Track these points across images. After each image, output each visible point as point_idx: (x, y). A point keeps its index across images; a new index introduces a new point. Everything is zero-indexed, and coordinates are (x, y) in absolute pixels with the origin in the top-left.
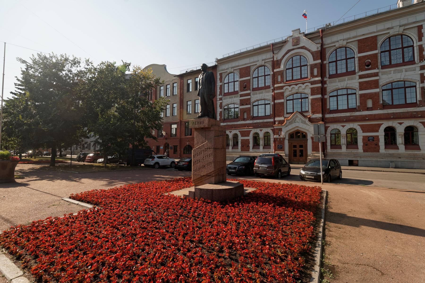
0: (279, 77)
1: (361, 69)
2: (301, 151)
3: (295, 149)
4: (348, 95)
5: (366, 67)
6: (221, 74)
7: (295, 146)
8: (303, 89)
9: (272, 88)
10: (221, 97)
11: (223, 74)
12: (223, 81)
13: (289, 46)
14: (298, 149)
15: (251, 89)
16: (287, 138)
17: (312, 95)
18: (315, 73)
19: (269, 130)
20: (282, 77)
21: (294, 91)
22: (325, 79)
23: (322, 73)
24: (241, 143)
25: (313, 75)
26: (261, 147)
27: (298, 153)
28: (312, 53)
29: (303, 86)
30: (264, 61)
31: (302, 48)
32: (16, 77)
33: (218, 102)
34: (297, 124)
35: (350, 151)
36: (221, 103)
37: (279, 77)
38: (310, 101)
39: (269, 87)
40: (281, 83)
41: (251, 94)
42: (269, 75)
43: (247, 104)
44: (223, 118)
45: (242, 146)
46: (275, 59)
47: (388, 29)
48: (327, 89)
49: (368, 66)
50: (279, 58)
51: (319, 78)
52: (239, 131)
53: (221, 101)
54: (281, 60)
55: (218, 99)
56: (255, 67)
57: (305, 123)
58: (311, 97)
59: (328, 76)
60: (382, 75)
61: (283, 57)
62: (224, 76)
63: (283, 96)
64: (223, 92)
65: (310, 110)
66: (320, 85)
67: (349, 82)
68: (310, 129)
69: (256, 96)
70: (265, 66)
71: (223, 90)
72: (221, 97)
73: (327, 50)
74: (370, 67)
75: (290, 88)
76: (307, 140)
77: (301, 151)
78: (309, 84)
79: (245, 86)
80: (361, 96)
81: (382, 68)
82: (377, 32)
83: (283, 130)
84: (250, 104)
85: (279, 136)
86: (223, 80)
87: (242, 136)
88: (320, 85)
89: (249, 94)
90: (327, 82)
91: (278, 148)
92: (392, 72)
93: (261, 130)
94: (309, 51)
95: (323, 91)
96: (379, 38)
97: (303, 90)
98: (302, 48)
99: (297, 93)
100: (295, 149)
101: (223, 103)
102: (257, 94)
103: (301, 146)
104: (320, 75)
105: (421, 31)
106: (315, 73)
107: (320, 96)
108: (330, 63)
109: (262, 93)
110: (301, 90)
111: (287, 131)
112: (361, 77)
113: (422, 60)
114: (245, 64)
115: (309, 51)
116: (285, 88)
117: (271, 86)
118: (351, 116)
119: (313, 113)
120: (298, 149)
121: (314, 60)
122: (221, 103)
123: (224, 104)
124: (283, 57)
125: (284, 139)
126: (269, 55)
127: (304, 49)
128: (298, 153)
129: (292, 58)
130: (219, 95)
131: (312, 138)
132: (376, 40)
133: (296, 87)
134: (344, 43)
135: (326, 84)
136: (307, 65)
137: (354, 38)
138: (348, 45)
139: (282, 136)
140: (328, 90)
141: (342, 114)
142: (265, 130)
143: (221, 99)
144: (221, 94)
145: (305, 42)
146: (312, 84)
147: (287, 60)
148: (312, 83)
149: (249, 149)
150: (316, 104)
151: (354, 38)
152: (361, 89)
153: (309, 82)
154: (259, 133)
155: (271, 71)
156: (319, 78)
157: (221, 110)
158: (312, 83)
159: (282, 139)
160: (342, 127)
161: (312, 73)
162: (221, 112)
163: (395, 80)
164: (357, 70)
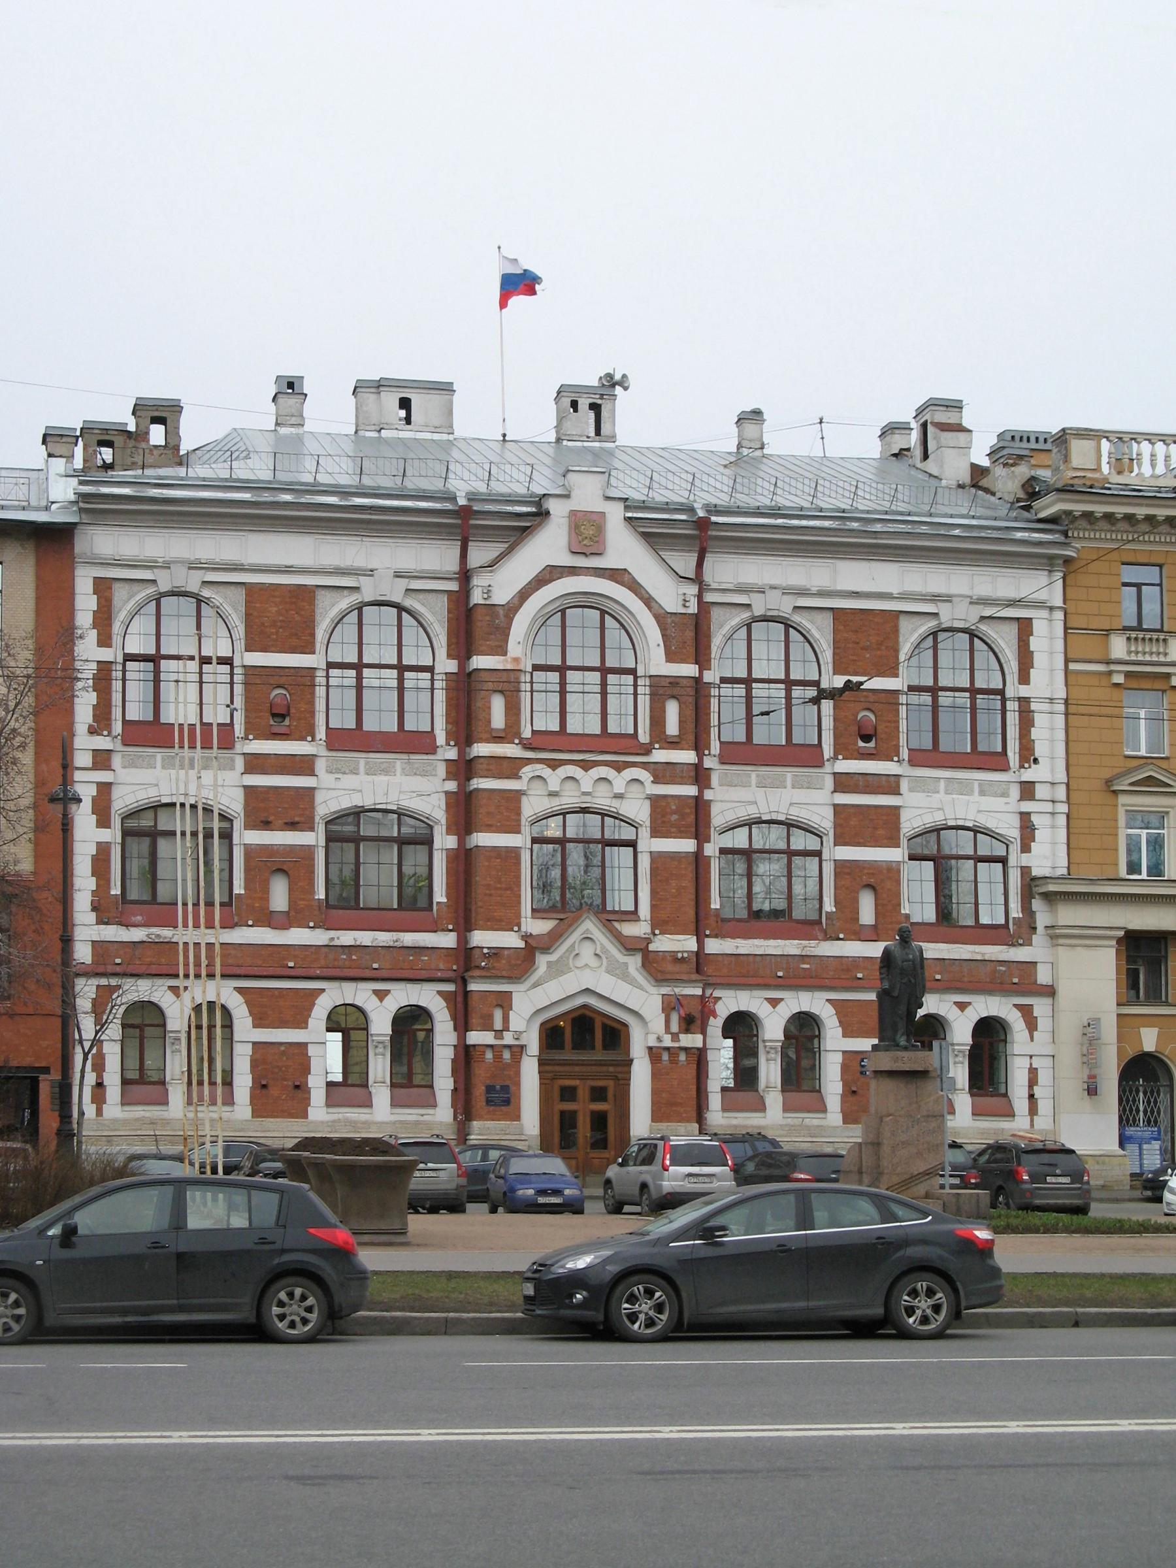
0: (498, 705)
1: (843, 749)
2: (599, 1121)
3: (569, 1106)
4: (791, 854)
5: (861, 744)
6: (102, 587)
7: (568, 1094)
8: (619, 796)
9: (452, 754)
10: (102, 742)
11: (119, 594)
12: (117, 640)
13: (548, 546)
14: (584, 1107)
15: (321, 733)
16: (534, 1047)
17: (657, 831)
18: (672, 727)
19: (428, 997)
20: (513, 710)
21: (570, 799)
22: (708, 763)
23: (696, 733)
24: (255, 1064)
25: (659, 737)
26: (177, 1094)
27: (584, 1129)
28: (662, 618)
29: (620, 780)
30: (403, 584)
31: (617, 575)
32: (1032, 1039)
33: (78, 776)
34: (587, 980)
35: (795, 1118)
36: (105, 789)
37: (498, 705)
38: (645, 863)
39: (422, 743)
40: (498, 738)
41: (320, 766)
42: (430, 669)
43: (292, 826)
44: (116, 891)
45: (260, 1087)
46: (477, 597)
47: (935, 598)
48: (715, 810)
49: (866, 738)
50: (502, 596)
51: (687, 756)
52: (239, 990)
53: (103, 776)
54: (512, 609)
55: (82, 759)
56: (346, 602)
57: (625, 977)
58: (650, 844)
59: (715, 747)
60: (911, 790)
61: (524, 595)
62: (124, 602)
63: (518, 812)
64: (117, 713)
65: (645, 911)
66: (691, 790)
67: (800, 795)
68: (643, 1007)
69: (349, 781)
70: (400, 608)
71: (116, 698)
72: (102, 742)
73: (716, 614)
74: (872, 744)
75: (554, 778)
76: (630, 1062)
77: (599, 1121)
78: (645, 776)
79: (279, 706)
80: (844, 869)
81: (913, 763)
82: (904, 597)
83: (516, 1000)
84: (312, 829)
85: (499, 1034)
86: (117, 627)
87: (260, 1021)
88: (691, 790)
89: (304, 765)
90: (715, 779)
91: (489, 1102)
92: (942, 784)
93: (381, 995)
94: (648, 601)
95: (695, 818)
96: (904, 624)
97: (616, 803)
98: (617, 575)
99: (584, 811)
100: (569, 1106)
101: (116, 793)
102: (355, 772)
103: (599, 1094)
104: (692, 737)
105: (1028, 644)
106: (672, 727)
107: (687, 845)
108: (724, 680)
109: (386, 772)
110: (602, 800)
111: (539, 1011)
112: (843, 783)
113: (1028, 762)
114: (287, 570)
115: (648, 601)
116: (527, 771)
117: (441, 738)
118: (803, 958)
119: (660, 924)
120: (584, 1107)
121: (671, 657)
122: (105, 789)
123: (123, 800)
124: (524, 595)
125: (518, 1051)
126: (439, 557)
127: (622, 584)
128: (584, 1129)
129: (563, 612)
130: (92, 731)
131: (654, 1054)
132: (896, 630)
133: (587, 779)
134: (784, 606)
135: (709, 787)
136: (633, 672)
137: (822, 594)
138: (797, 618)
139: (508, 1039)
140: (719, 816)
141: (772, 942)
142: (403, 995)
143: (102, 760)
144: (101, 721)
145: (624, 548)
146: (657, 780)
147: (543, 620)
148: (663, 773)
149: (306, 1101)
150: (673, 883)
151: (822, 594)
152: (840, 841)
153: (645, 766)
154: (368, 1007)
155: (442, 652)
156: (687, 756)
157: (105, 835)
158: (663, 773)
159: (507, 1055)
160: (767, 1006)
161: (658, 721)
162: (103, 851)
163: (951, 823)
164: (828, 750)
